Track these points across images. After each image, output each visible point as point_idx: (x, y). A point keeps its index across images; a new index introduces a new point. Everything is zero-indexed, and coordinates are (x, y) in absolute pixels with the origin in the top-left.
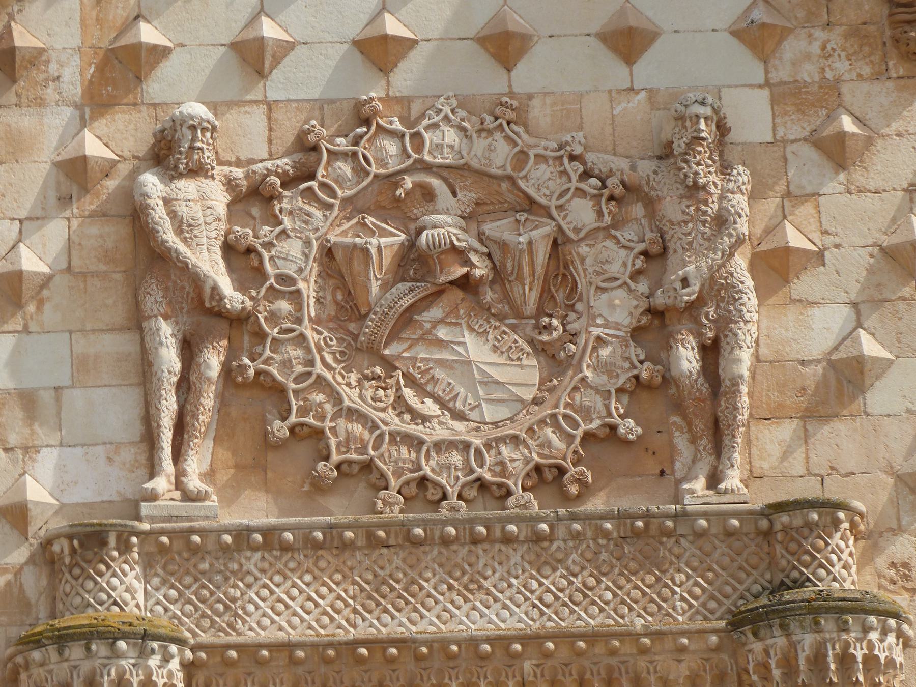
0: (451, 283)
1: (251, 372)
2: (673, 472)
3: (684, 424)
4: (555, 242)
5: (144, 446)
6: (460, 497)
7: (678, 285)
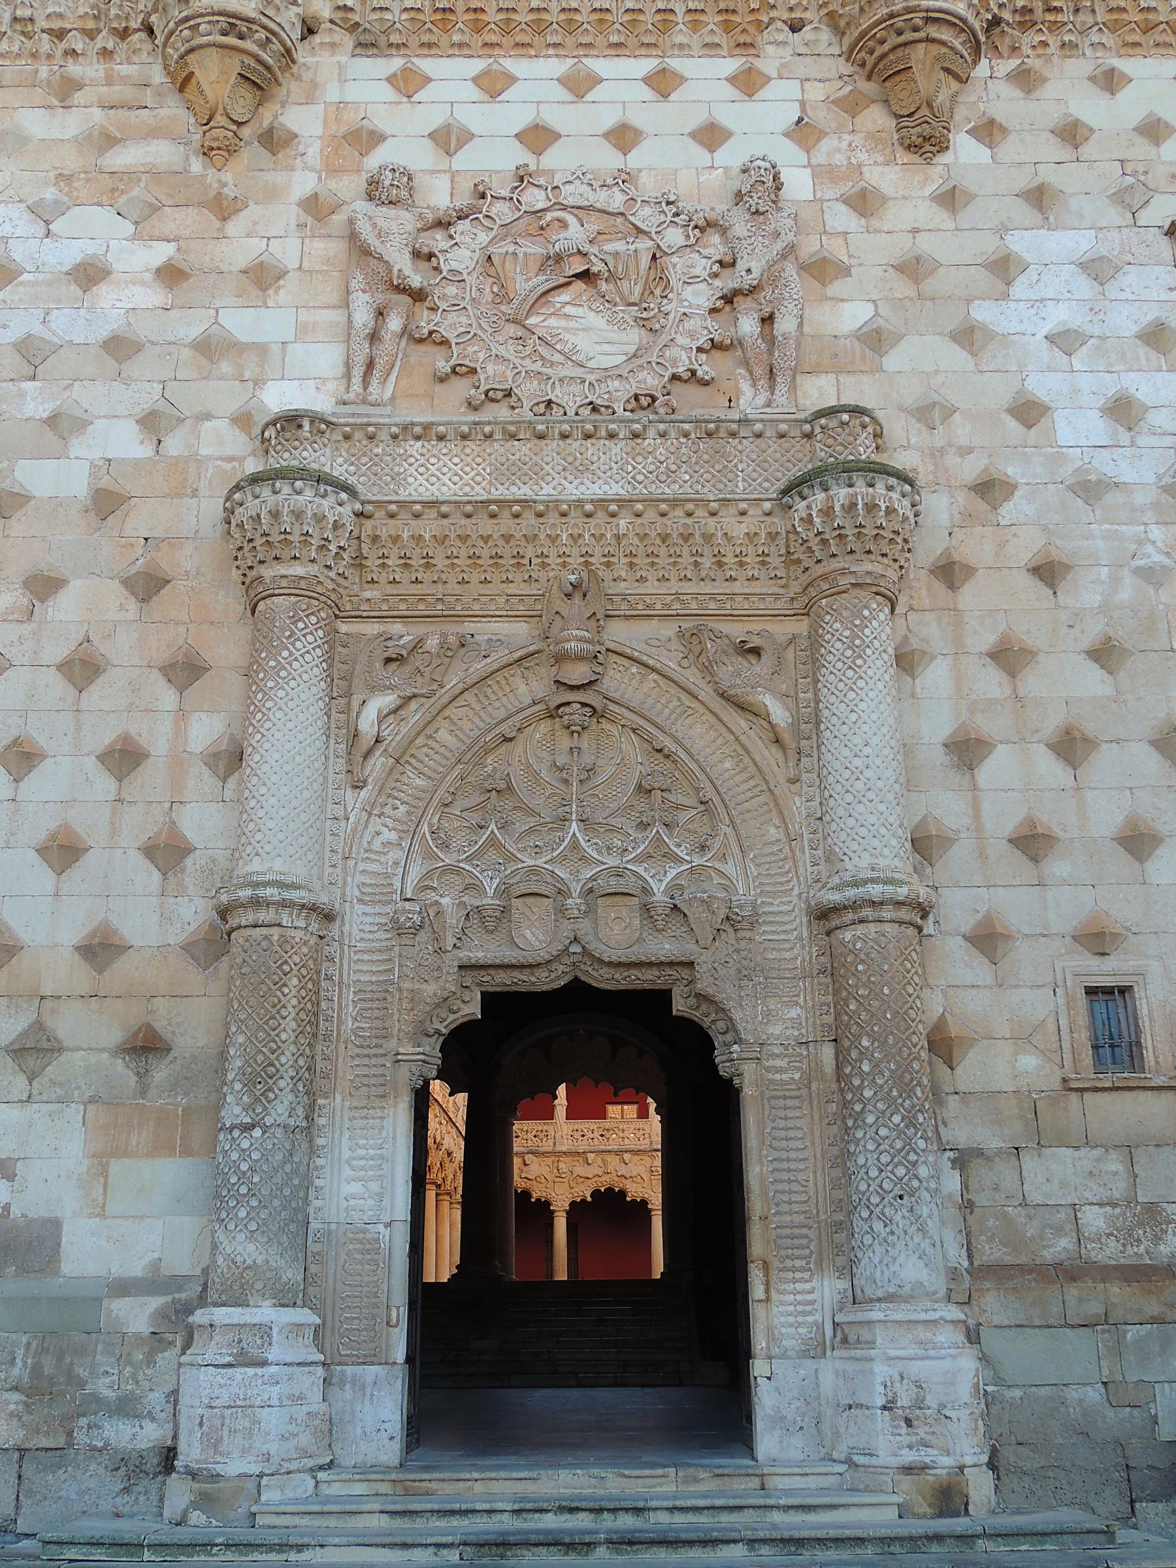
0: (577, 276)
1: (426, 331)
2: (738, 405)
3: (747, 374)
4: (654, 257)
5: (344, 381)
6: (577, 414)
7: (743, 274)
